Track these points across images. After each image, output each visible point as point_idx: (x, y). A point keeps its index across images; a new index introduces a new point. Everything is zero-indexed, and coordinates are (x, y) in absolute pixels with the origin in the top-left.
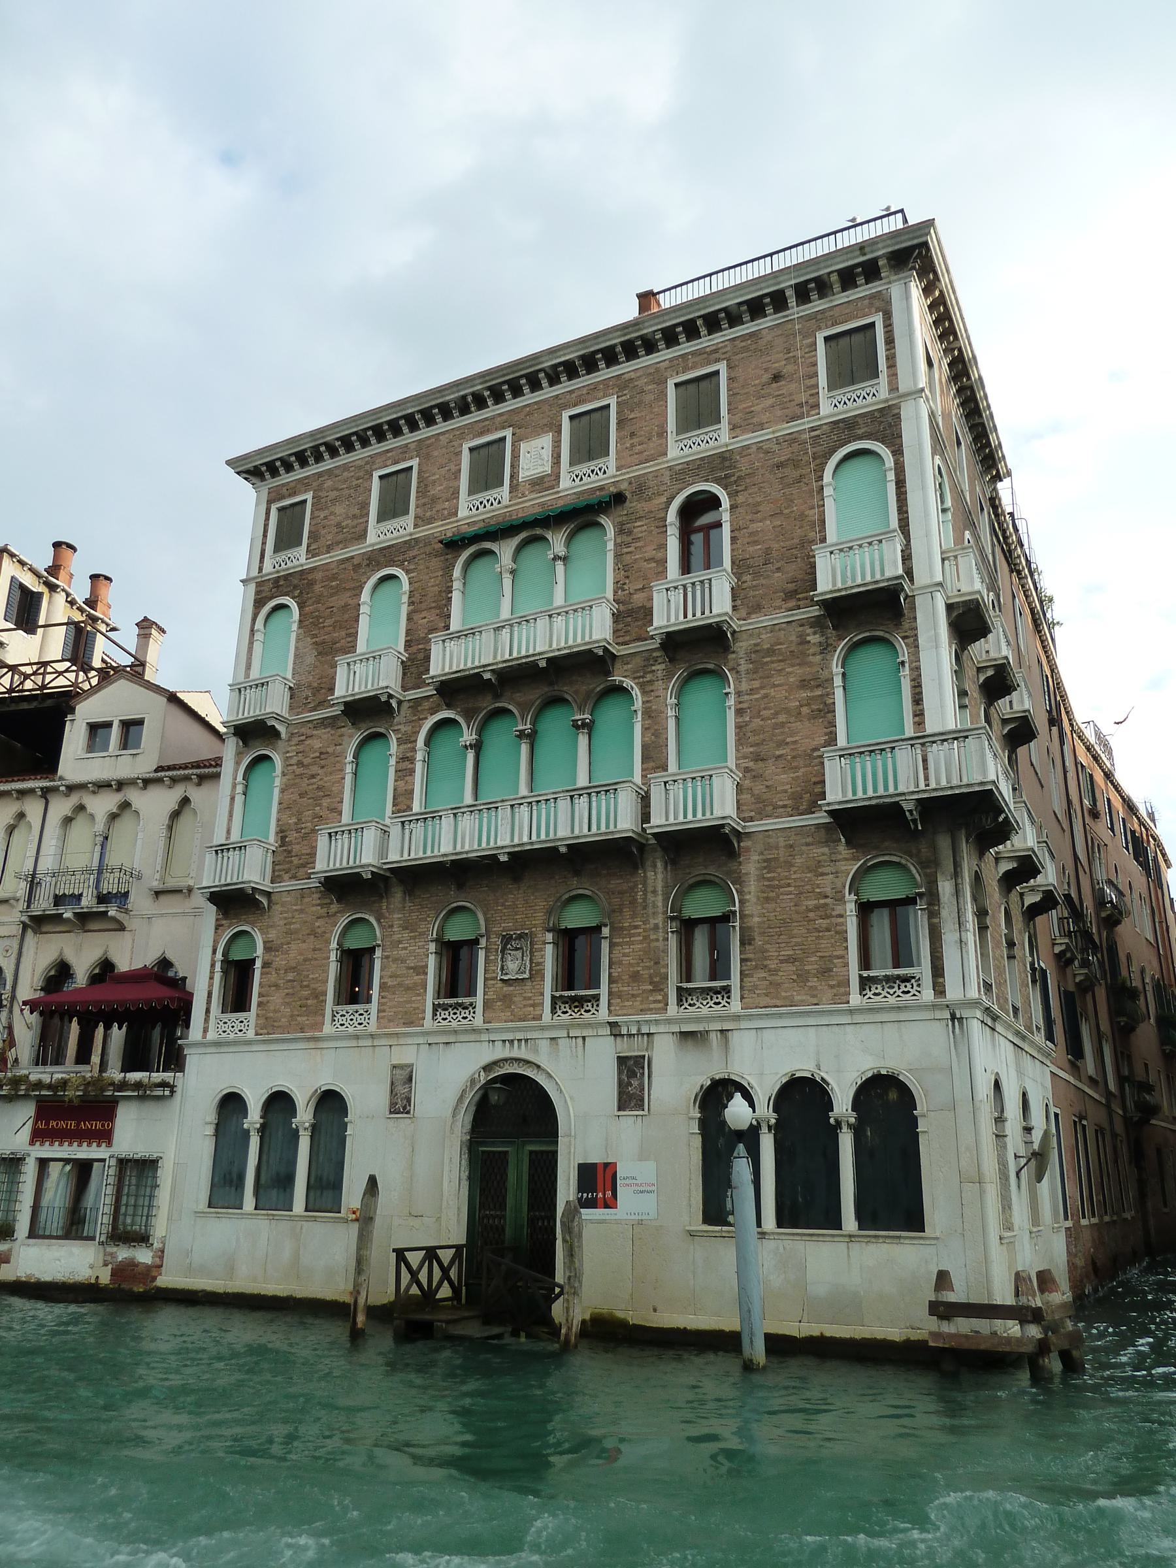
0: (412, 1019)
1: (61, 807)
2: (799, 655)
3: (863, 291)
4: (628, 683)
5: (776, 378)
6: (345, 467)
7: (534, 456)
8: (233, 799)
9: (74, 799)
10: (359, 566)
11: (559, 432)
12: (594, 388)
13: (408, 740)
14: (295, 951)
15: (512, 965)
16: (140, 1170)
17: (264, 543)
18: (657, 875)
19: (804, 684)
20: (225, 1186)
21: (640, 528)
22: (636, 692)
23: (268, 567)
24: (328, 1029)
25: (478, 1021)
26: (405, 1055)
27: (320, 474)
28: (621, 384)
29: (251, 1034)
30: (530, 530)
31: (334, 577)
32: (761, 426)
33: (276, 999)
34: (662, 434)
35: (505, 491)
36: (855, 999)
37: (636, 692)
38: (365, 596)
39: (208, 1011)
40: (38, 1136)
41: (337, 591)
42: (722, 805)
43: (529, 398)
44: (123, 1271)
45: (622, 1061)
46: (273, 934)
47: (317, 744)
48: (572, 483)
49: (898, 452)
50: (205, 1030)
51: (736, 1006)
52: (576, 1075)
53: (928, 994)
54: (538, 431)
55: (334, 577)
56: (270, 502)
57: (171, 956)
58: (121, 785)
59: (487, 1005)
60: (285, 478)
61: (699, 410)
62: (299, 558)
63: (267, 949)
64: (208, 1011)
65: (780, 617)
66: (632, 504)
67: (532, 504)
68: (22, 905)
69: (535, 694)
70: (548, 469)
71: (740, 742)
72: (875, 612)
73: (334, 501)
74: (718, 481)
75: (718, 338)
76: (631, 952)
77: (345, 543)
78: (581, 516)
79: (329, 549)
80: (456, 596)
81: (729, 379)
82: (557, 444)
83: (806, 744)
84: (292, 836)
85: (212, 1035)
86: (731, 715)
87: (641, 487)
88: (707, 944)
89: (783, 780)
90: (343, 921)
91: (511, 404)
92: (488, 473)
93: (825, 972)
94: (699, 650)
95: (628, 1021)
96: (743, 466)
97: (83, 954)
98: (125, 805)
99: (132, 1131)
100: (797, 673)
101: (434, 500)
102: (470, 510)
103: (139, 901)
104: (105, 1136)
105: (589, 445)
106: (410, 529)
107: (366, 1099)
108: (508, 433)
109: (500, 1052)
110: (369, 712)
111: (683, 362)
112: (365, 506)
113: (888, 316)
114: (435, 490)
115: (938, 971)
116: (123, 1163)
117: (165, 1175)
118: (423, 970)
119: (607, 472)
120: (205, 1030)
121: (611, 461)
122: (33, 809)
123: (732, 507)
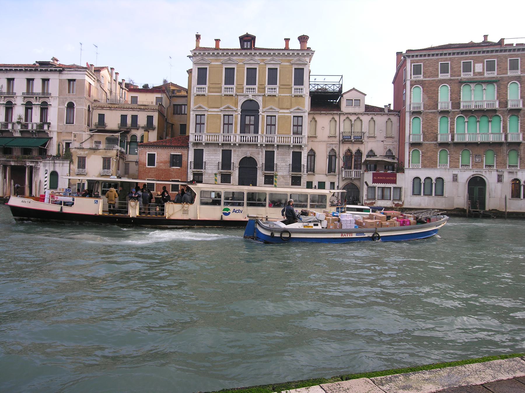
0: (457, 167)
1: (343, 118)
4: (500, 115)
8: (410, 125)
9: (346, 116)
10: (437, 82)
11: (484, 63)
12: (492, 56)
13: (453, 119)
14: (429, 154)
15: (477, 160)
17: (411, 72)
18: (505, 148)
20: (416, 192)
21: (502, 87)
22: (501, 117)
24: (438, 167)
25: (471, 168)
26: (455, 172)
27: (424, 60)
28: (497, 57)
29: (420, 167)
30: (480, 82)
31: (431, 83)
33: (426, 162)
34: (507, 69)
35: (472, 73)
37: (501, 117)
38: (439, 89)
39: (409, 163)
44: (397, 205)
45: (498, 175)
46: (423, 151)
47: (430, 117)
48: (487, 75)
50: (409, 166)
51: (519, 168)
52: (490, 177)
55: (431, 83)
56: (411, 63)
57: (373, 149)
58: (358, 114)
59: (472, 166)
60: (415, 58)
61: (514, 66)
62: (421, 77)
63: (422, 153)
64: (409, 163)
66: (501, 82)
68: (338, 138)
71: (521, 128)
73: (429, 66)
74: (518, 81)
75: (519, 53)
78: (490, 82)
79: (429, 77)
80: (461, 92)
81: (521, 62)
82: (483, 66)
85: (411, 167)
86: (519, 124)
88: (512, 158)
90: (440, 150)
92: (467, 68)
94: (515, 112)
95: (500, 170)
96: (523, 79)
97: (354, 149)
98: (358, 118)
101: (455, 72)
102: (464, 76)
103: (365, 139)
105: (490, 67)
108: (472, 61)
109: (475, 173)
111: (511, 56)
118: (459, 159)
119: (495, 74)
120: (409, 166)
121: (496, 72)
122: (337, 118)
123: (521, 87)
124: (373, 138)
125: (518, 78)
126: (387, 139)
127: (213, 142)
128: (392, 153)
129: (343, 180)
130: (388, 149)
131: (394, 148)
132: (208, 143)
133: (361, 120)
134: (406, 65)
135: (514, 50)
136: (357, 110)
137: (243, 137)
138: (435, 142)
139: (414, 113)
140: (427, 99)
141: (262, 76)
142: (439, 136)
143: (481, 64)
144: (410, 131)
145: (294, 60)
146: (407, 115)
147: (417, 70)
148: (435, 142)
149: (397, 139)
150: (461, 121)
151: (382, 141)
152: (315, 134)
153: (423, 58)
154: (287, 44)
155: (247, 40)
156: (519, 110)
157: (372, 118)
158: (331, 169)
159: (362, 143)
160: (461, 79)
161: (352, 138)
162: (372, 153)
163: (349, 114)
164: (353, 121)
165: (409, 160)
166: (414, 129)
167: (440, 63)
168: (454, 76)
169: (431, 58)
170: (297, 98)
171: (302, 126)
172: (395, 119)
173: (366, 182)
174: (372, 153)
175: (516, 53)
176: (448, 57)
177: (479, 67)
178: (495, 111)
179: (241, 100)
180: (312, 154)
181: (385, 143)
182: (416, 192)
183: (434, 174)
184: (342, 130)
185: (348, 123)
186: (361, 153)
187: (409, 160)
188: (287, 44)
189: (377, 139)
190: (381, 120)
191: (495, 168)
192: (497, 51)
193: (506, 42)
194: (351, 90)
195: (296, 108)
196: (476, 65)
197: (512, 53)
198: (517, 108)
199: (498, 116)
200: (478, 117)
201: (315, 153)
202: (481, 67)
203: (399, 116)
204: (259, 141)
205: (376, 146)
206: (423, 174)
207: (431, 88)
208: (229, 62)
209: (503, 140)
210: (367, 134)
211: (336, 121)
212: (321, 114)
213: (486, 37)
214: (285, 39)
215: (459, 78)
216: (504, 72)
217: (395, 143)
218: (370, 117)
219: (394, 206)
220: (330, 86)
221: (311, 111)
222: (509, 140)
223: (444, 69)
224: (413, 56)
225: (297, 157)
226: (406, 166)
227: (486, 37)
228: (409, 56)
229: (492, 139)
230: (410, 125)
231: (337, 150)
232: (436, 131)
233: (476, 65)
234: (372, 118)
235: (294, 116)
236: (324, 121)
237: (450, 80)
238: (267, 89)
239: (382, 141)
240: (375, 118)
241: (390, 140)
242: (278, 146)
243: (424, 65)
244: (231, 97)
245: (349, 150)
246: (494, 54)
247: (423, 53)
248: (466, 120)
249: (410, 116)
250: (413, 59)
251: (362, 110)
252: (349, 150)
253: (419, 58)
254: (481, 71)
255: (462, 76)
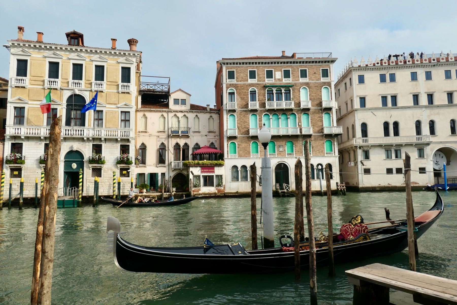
1: (171, 115)
2: (318, 113)
3: (327, 64)
5: (315, 73)
6: (242, 67)
7: (278, 75)
9: (174, 114)
10: (247, 86)
16: (220, 177)
18: (301, 139)
19: (319, 117)
20: (235, 178)
21: (296, 91)
23: (228, 82)
24: (251, 157)
25: (276, 156)
29: (237, 157)
32: (313, 80)
33: (241, 152)
34: (299, 77)
36: (326, 155)
37: (297, 115)
39: (228, 153)
40: (202, 172)
41: (243, 89)
42: (311, 132)
43: (276, 65)
49: (331, 89)
50: (228, 156)
53: (333, 155)
54: (278, 71)
55: (242, 86)
56: (226, 69)
57: (198, 143)
60: (229, 65)
61: (304, 74)
63: (238, 145)
64: (228, 153)
65: (316, 108)
66: (294, 87)
67: (278, 83)
68: (167, 133)
69: (282, 112)
70: (280, 78)
72: (328, 110)
75: (306, 64)
76: (297, 148)
77: (244, 81)
79: (241, 81)
83: (319, 125)
84: (240, 128)
85: (229, 157)
87: (296, 84)
89: (317, 129)
91: (273, 65)
93: (322, 152)
94: (306, 111)
96: (311, 85)
97: (182, 142)
98: (185, 115)
99: (218, 171)
100: (318, 115)
101: (260, 78)
104: (214, 172)
105: (287, 74)
106: (256, 82)
107: (259, 165)
110: (254, 111)
112: (247, 75)
113: (330, 69)
114: (260, 76)
115: (334, 152)
116: (217, 176)
117: (224, 177)
120: (228, 156)
122: (165, 114)
124: (198, 133)
125: (307, 84)
126: (210, 134)
127: (34, 135)
128: (215, 146)
129: (173, 171)
130: (210, 143)
131: (216, 141)
132: (28, 137)
133: (187, 117)
134: (222, 71)
135: (303, 62)
136: (183, 108)
137: (68, 130)
138: (247, 136)
139: (230, 111)
140: (240, 100)
141: (89, 72)
142: (250, 131)
143: (280, 73)
144: (227, 126)
145: (122, 59)
146: (225, 113)
147: (231, 75)
148: (247, 136)
149: (217, 133)
150: (267, 117)
151: (206, 135)
152: (146, 129)
153: (235, 65)
154: (114, 44)
155: (75, 38)
156: (308, 109)
157: (197, 116)
158: (161, 160)
159: (188, 137)
160: (265, 84)
161: (180, 133)
162: (197, 146)
163: (177, 111)
164: (180, 117)
165: (228, 151)
166: (230, 125)
167: (249, 70)
168: (260, 81)
169: (242, 65)
170: (124, 94)
171: (129, 121)
172: (215, 116)
173: (192, 172)
174: (197, 146)
175: (305, 64)
176: (254, 65)
177: (278, 75)
178: (291, 110)
179: (67, 94)
180: (143, 148)
181: (208, 137)
182: (235, 178)
183: (248, 163)
184: (170, 126)
185: (175, 120)
186: (188, 146)
187: (228, 151)
188: (114, 44)
189: (201, 134)
190: (204, 117)
191: (294, 156)
192: (291, 62)
193: (297, 56)
194: (177, 91)
195: (124, 103)
196: (276, 73)
197: (302, 64)
198: (307, 107)
199: (294, 114)
200: (280, 114)
201: (146, 146)
202: (280, 75)
203: (219, 114)
204: (85, 135)
205: (199, 139)
206: (239, 163)
207: (243, 91)
208: (54, 56)
209: (299, 133)
210: (192, 130)
211: (165, 118)
212: (151, 111)
213: (283, 52)
214: (112, 39)
215: (264, 83)
216: (297, 79)
217: (216, 137)
218: (195, 114)
219: (216, 192)
220: (159, 86)
221: (142, 108)
222: (303, 133)
223: (252, 75)
224: (227, 64)
225: (125, 149)
226: (226, 156)
227: (283, 52)
228: (224, 64)
229: (291, 132)
230: (227, 121)
231: (166, 143)
232: (248, 126)
233: (276, 73)
234: (197, 116)
235: (122, 112)
236: (155, 118)
237: (258, 84)
238: (93, 84)
239: (206, 135)
240: (199, 115)
241: (212, 134)
242: (105, 139)
243: (237, 72)
244: (55, 91)
245: (177, 144)
246: (289, 64)
247: (236, 61)
248: (271, 117)
249: (227, 113)
250: (227, 66)
251: (187, 107)
252: (177, 144)
253: (232, 65)
254: (280, 78)
255: (266, 81)
